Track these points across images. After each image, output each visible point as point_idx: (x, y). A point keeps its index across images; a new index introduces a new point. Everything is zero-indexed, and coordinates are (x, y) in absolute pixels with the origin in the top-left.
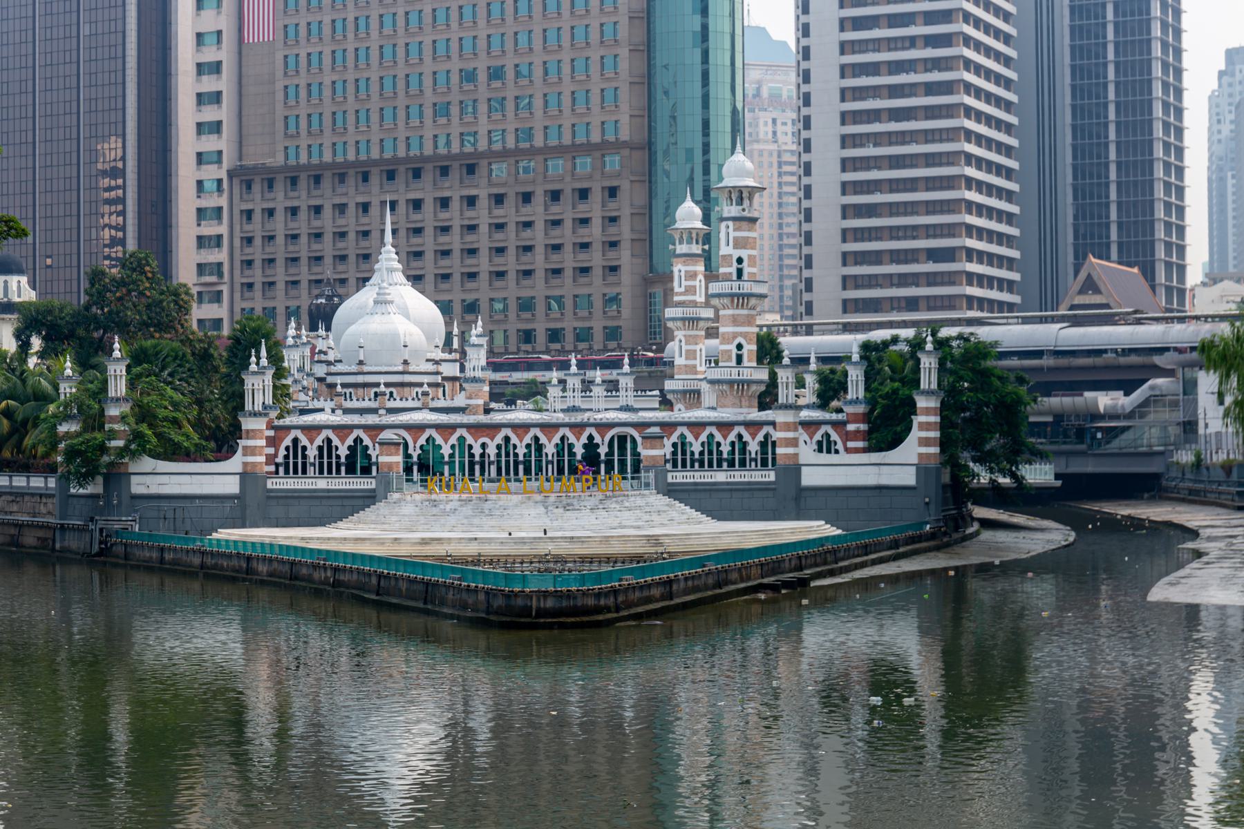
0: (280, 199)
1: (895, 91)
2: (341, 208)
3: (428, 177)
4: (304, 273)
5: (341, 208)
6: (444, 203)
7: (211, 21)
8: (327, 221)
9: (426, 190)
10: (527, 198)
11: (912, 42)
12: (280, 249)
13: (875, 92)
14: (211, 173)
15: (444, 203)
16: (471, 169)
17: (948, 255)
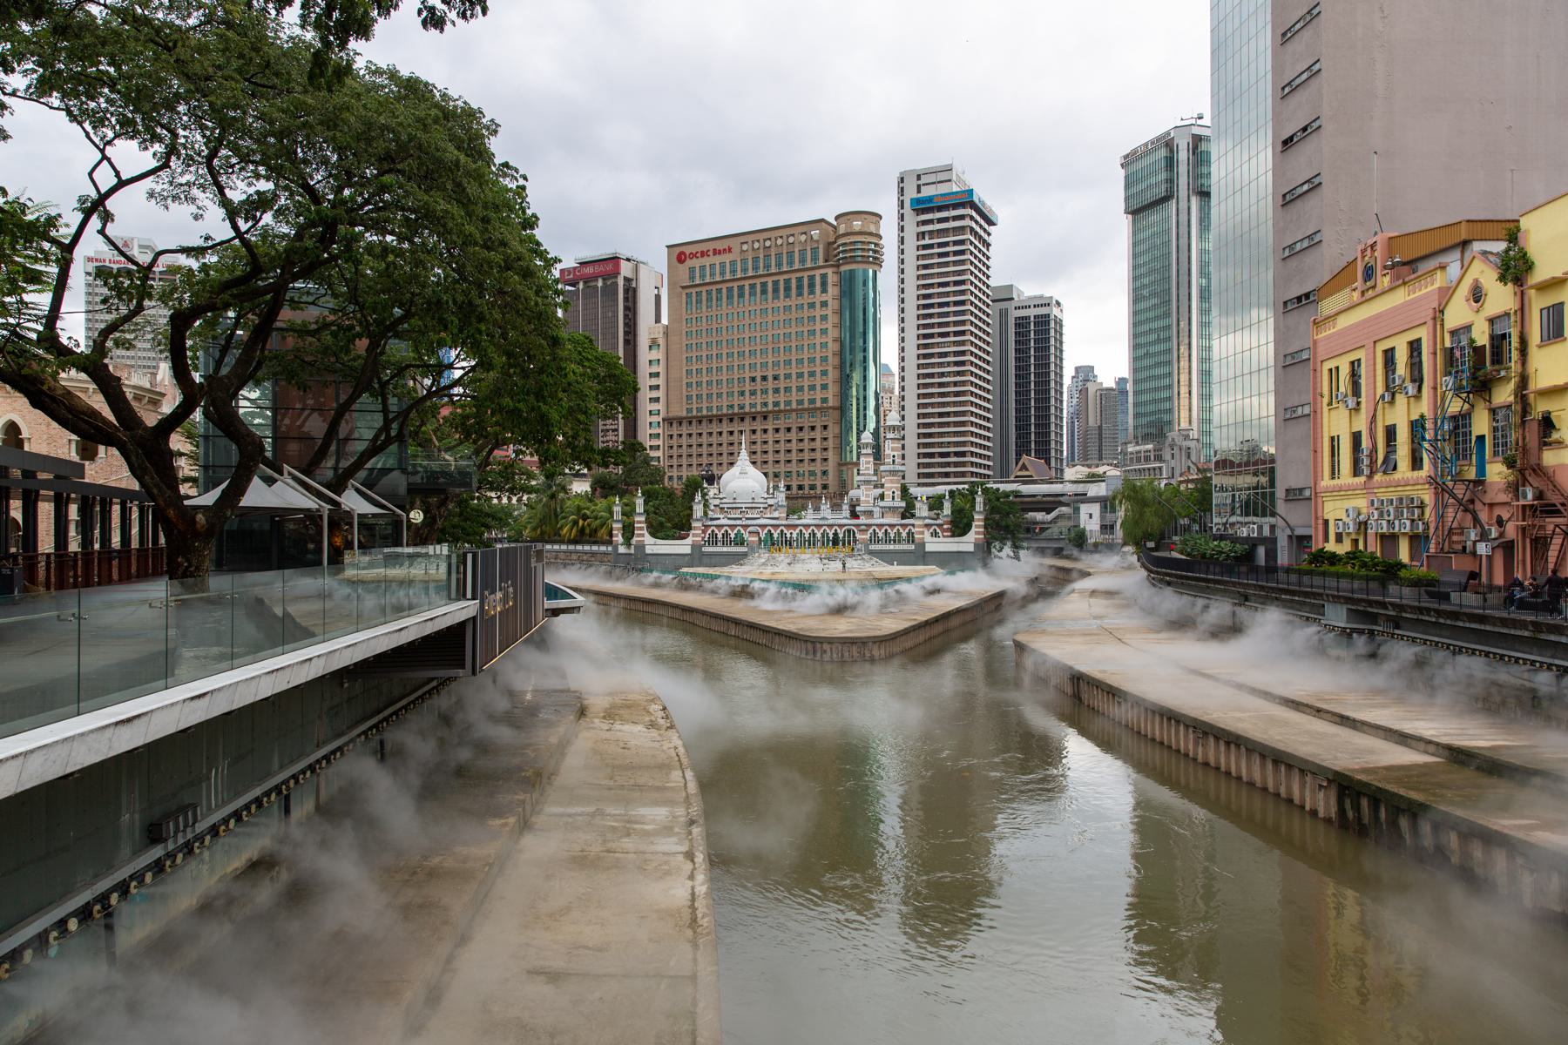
0: (685, 430)
1: (941, 385)
2: (710, 434)
3: (747, 420)
4: (694, 461)
5: (710, 434)
7: (654, 355)
8: (704, 439)
11: (949, 364)
12: (684, 451)
13: (932, 385)
14: (655, 419)
17: (963, 454)
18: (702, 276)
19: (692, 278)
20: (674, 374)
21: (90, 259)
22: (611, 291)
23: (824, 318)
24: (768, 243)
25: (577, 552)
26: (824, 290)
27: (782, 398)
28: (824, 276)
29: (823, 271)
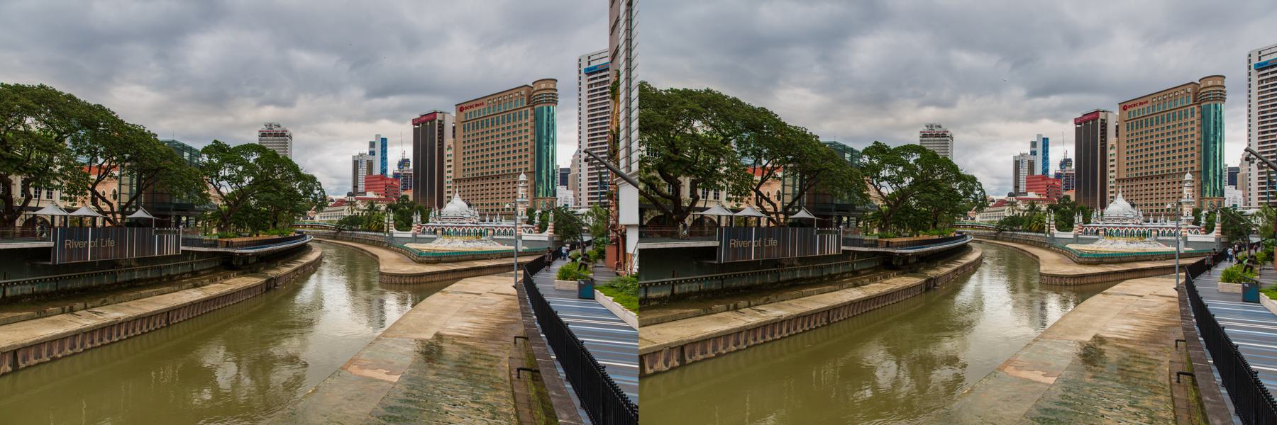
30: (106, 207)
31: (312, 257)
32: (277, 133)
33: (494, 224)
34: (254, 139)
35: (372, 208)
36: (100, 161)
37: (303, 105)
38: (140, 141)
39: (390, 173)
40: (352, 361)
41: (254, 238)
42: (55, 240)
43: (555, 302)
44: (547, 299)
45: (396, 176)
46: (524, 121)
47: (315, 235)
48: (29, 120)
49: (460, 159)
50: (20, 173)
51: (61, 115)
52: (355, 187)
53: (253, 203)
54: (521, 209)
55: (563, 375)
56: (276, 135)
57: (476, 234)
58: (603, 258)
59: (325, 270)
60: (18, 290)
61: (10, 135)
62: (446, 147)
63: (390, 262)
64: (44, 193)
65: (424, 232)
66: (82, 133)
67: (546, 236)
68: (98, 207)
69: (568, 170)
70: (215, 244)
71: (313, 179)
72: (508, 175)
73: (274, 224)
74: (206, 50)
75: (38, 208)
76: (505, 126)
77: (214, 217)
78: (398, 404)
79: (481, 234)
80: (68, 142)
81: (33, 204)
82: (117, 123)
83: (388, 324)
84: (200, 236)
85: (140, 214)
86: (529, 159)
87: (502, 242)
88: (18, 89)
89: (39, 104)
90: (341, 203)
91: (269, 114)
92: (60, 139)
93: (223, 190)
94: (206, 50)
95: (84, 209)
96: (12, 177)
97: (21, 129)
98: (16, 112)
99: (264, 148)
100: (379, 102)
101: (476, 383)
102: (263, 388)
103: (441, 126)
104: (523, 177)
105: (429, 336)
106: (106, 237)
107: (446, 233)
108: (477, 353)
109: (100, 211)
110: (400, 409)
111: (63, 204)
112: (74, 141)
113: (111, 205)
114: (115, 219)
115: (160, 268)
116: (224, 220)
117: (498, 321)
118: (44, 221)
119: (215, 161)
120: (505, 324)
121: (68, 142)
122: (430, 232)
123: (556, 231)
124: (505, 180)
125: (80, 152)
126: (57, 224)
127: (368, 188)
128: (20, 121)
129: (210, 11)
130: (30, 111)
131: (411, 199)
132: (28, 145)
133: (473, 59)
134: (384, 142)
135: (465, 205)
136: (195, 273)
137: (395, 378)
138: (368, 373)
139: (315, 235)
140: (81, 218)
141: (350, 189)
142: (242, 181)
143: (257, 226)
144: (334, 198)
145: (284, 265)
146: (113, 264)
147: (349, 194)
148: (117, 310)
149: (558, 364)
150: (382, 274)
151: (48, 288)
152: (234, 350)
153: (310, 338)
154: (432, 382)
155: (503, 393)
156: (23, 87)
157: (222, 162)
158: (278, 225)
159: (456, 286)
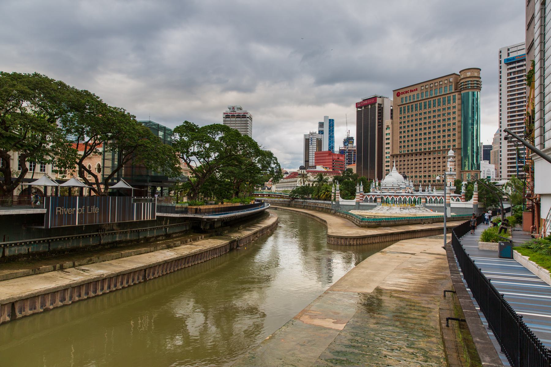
2: (408, 160)
3: (422, 155)
5: (408, 160)
6: (425, 159)
8: (406, 163)
9: (422, 157)
10: (439, 158)
14: (388, 155)
15: (425, 159)
16: (430, 154)
18: (406, 101)
19: (402, 102)
20: (395, 139)
21: (224, 113)
22: (373, 109)
23: (454, 113)
24: (432, 86)
25: (325, 203)
26: (454, 102)
27: (436, 145)
28: (454, 96)
29: (454, 94)
30: (91, 179)
31: (270, 222)
32: (239, 115)
33: (426, 193)
34: (219, 120)
35: (321, 179)
36: (87, 139)
37: (262, 91)
38: (120, 122)
39: (336, 149)
40: (304, 312)
41: (220, 205)
42: (47, 207)
43: (479, 261)
44: (472, 258)
45: (342, 152)
46: (452, 105)
47: (272, 203)
48: (25, 104)
49: (397, 137)
50: (17, 149)
51: (53, 100)
52: (307, 161)
53: (218, 175)
54: (450, 181)
55: (486, 324)
56: (238, 116)
57: (410, 202)
58: (521, 223)
59: (281, 233)
60: (16, 251)
61: (9, 116)
62: (385, 127)
63: (336, 227)
64: (38, 166)
65: (366, 200)
66: (71, 115)
67: (471, 204)
68: (85, 179)
69: (490, 147)
70: (186, 211)
71: (270, 155)
72: (439, 151)
73: (237, 194)
74: (178, 43)
75: (33, 180)
76: (436, 109)
77: (185, 187)
78: (344, 349)
79: (415, 202)
80: (59, 123)
81: (28, 176)
82: (101, 106)
83: (335, 280)
84: (173, 203)
85: (121, 184)
86: (456, 138)
87: (433, 209)
88: (16, 77)
89: (34, 90)
90: (294, 175)
91: (232, 98)
92: (52, 120)
93: (192, 164)
94: (178, 43)
95: (73, 181)
96: (10, 153)
97: (19, 111)
98: (14, 97)
99: (228, 128)
100: (327, 88)
101: (411, 331)
102: (227, 335)
103: (381, 109)
104: (451, 153)
105: (370, 290)
106: (91, 204)
107: (385, 202)
108: (412, 305)
109: (86, 182)
110: (344, 353)
111: (54, 177)
112: (64, 122)
113: (95, 177)
114: (99, 189)
115: (138, 232)
116: (193, 190)
117: (429, 277)
118: (38, 191)
119: (186, 139)
120: (436, 280)
121: (59, 123)
122: (371, 200)
123: (480, 199)
124: (436, 155)
125: (69, 131)
126: (49, 193)
127: (318, 162)
128: (17, 104)
129: (181, 9)
130: (26, 96)
131: (355, 171)
132: (24, 125)
133: (408, 51)
134: (331, 123)
135: (401, 177)
136: (168, 236)
137: (341, 327)
138: (317, 322)
139: (272, 203)
140: (70, 188)
141: (302, 163)
142: (209, 157)
143: (222, 195)
144: (288, 171)
145: (245, 229)
146: (98, 228)
147: (301, 168)
148: (101, 268)
149: (481, 314)
150: (329, 236)
151: (41, 249)
152: (203, 302)
153: (268, 292)
154: (372, 330)
155: (434, 340)
156: (20, 75)
157: (192, 140)
158: (240, 194)
159: (394, 247)
